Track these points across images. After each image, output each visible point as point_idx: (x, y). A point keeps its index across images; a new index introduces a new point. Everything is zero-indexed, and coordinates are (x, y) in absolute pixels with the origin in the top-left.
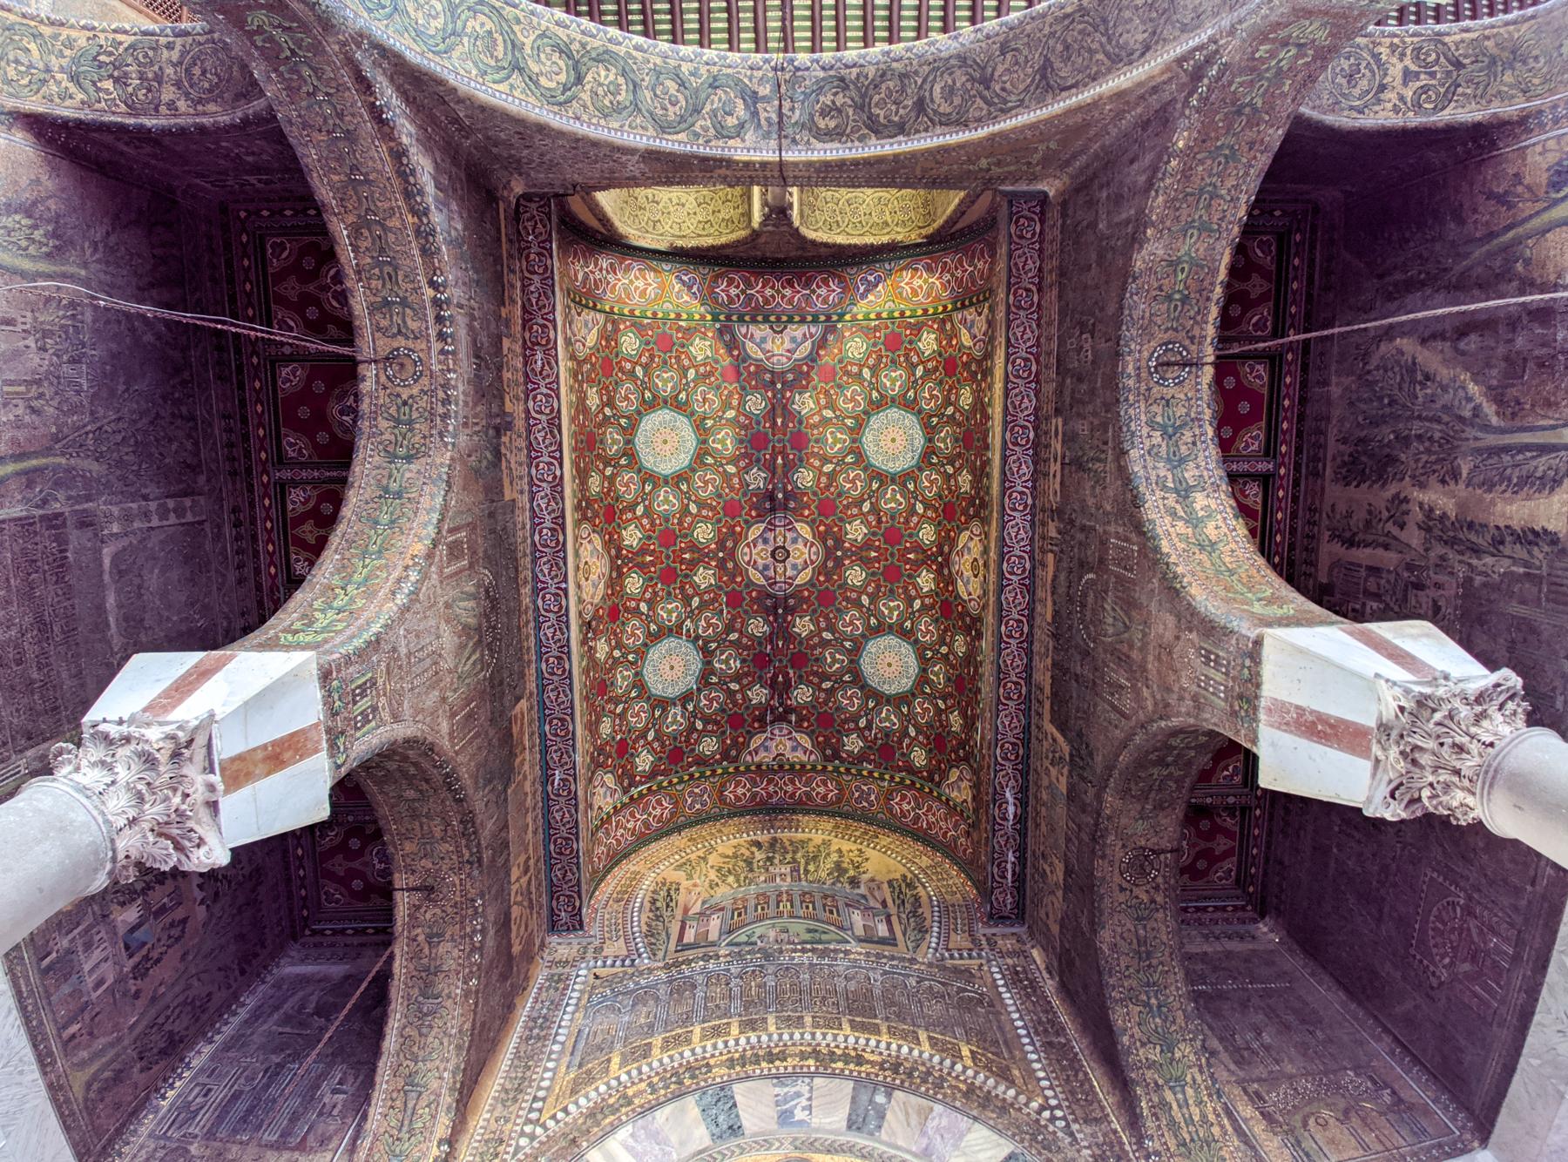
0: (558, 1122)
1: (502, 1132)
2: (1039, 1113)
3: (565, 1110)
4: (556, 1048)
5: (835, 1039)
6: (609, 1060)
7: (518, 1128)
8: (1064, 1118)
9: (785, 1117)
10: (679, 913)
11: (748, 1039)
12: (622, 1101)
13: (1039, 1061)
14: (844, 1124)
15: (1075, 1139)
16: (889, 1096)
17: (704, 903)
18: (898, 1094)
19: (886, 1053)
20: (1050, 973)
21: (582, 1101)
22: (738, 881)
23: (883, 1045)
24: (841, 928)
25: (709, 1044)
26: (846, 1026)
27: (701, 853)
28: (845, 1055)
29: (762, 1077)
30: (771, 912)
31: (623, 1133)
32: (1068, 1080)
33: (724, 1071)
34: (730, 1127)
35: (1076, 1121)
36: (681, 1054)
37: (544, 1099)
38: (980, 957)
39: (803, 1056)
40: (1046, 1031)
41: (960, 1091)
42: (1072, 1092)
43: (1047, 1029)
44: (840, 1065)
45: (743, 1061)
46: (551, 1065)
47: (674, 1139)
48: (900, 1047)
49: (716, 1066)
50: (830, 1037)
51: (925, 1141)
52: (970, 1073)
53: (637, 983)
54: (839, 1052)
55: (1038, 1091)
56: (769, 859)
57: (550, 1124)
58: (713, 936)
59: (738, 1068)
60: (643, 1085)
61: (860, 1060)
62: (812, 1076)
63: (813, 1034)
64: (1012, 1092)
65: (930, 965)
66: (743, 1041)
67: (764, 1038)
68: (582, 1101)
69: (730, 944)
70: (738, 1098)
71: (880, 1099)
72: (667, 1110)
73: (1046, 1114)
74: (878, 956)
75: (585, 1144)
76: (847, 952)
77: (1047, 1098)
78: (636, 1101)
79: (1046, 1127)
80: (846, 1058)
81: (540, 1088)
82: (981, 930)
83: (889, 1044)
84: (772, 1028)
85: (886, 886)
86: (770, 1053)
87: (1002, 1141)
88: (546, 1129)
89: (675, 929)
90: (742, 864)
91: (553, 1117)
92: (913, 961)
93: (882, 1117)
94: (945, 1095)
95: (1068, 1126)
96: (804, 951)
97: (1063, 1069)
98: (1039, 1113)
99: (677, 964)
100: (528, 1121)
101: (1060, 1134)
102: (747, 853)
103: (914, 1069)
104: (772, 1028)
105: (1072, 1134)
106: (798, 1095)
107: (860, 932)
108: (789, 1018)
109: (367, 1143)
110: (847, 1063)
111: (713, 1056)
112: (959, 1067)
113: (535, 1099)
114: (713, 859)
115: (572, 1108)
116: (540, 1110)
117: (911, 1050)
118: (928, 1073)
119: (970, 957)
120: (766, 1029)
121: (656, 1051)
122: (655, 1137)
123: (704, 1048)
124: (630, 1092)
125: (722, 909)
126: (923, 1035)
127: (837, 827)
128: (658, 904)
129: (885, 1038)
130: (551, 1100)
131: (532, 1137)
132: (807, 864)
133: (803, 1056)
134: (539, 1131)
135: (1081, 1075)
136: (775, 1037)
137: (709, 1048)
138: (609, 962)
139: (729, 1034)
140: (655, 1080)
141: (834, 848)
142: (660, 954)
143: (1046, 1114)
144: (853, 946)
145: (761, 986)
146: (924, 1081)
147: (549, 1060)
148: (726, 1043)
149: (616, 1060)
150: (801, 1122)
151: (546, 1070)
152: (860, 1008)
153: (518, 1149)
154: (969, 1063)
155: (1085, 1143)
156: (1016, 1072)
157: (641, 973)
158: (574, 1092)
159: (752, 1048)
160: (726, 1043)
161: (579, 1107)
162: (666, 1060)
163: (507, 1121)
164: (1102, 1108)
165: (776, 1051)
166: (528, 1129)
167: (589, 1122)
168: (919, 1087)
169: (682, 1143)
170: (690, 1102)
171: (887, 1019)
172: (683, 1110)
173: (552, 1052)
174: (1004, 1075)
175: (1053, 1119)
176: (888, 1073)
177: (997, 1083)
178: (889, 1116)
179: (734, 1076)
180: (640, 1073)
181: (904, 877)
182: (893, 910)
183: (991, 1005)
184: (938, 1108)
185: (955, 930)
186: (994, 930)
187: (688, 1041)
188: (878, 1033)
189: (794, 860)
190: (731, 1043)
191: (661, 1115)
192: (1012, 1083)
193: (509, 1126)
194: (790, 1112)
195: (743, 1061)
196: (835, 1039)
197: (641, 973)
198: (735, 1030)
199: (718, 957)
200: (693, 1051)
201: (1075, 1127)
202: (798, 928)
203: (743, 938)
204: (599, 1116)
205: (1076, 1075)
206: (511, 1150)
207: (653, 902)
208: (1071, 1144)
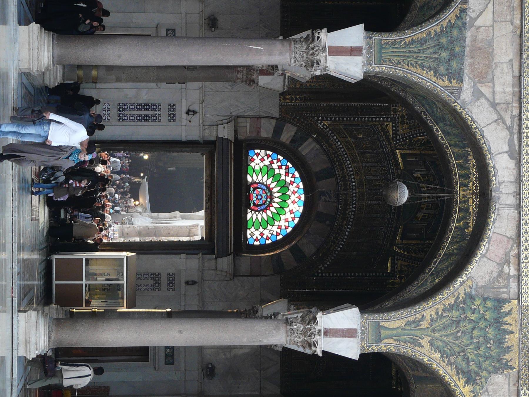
8: (318, 276)
9: (323, 193)
13: (340, 275)
31: (318, 146)
46: (345, 119)
49: (343, 173)
54: (347, 212)
64: (328, 263)
68: (330, 132)
70: (330, 179)
71: (328, 222)
73: (320, 271)
88: (320, 124)
89: (415, 152)
95: (315, 276)
100: (323, 118)
113: (331, 118)
115: (328, 130)
118: (337, 239)
134: (320, 122)
143: (320, 271)
151: (343, 119)
157: (389, 141)
161: (328, 132)
173: (350, 118)
175: (318, 273)
184: (323, 239)
191: (325, 157)
194: (324, 195)
197: (389, 141)
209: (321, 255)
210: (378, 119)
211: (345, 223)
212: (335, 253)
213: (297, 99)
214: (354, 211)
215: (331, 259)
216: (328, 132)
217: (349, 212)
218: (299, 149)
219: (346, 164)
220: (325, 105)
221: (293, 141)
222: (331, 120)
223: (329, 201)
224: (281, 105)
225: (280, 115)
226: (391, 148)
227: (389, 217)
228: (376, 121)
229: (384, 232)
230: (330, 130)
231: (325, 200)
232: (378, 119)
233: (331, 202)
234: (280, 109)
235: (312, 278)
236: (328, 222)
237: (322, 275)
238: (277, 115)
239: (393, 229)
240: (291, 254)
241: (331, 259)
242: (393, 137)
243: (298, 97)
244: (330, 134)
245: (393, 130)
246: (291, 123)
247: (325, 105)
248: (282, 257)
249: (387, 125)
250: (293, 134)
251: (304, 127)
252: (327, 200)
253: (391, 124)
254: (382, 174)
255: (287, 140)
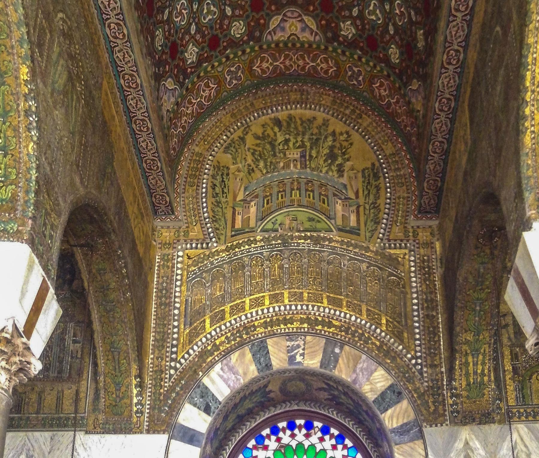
0: (186, 360)
1: (161, 366)
2: (410, 360)
3: (188, 353)
4: (176, 312)
5: (318, 310)
6: (204, 321)
7: (168, 364)
8: (421, 364)
9: (292, 359)
10: (230, 197)
11: (274, 308)
12: (214, 348)
13: (418, 328)
14: (319, 364)
15: (423, 377)
16: (341, 348)
17: (246, 189)
18: (347, 348)
19: (343, 320)
20: (441, 263)
21: (195, 348)
22: (266, 166)
23: (342, 315)
24: (329, 218)
25: (254, 311)
26: (325, 301)
27: (239, 133)
28: (323, 320)
29: (281, 334)
30: (287, 200)
32: (429, 341)
33: (262, 330)
34: (266, 365)
35: (426, 366)
36: (240, 318)
37: (176, 346)
38: (406, 248)
39: (302, 321)
40: (428, 307)
41: (376, 346)
42: (430, 349)
43: (429, 304)
44: (320, 327)
45: (272, 323)
46: (176, 324)
47: (241, 371)
48: (351, 316)
49: (258, 326)
50: (315, 308)
51: (354, 376)
52: (383, 334)
53: (212, 263)
54: (320, 319)
55: (413, 347)
56: (287, 141)
57: (183, 361)
58: (252, 223)
59: (269, 328)
60: (223, 338)
61: (330, 325)
62: (306, 334)
63: (307, 306)
65: (376, 253)
66: (271, 310)
67: (282, 308)
68: (195, 348)
69: (263, 231)
70: (270, 348)
71: (337, 350)
72: (237, 354)
74: (349, 244)
75: (201, 373)
76: (330, 240)
77: (416, 352)
78: (221, 348)
79: (411, 369)
80: (323, 323)
81: (174, 339)
82: (412, 222)
83: (346, 314)
84: (286, 301)
85: (360, 175)
86: (285, 319)
87: (389, 377)
88: (181, 364)
89: (229, 216)
90: (268, 146)
91: (183, 357)
92: (367, 249)
93: (337, 361)
94: (368, 348)
96: (306, 238)
97: (429, 333)
98: (410, 360)
99: (232, 248)
100: (172, 360)
101: (417, 373)
102: (272, 134)
103: (356, 331)
104: (286, 301)
105: (421, 373)
106: (298, 346)
107: (339, 222)
108: (295, 294)
109: (102, 378)
110: (323, 327)
111: (256, 319)
112: (378, 331)
113: (173, 346)
114: (250, 140)
115: (191, 351)
116: (176, 353)
117: (357, 318)
118: (363, 334)
119: (401, 248)
120: (283, 302)
121: (227, 315)
122: (231, 369)
123: (251, 313)
124: (218, 342)
125: (257, 197)
126: (364, 308)
127: (334, 102)
128: (218, 190)
129: (345, 310)
130: (180, 346)
131: (176, 369)
132: (311, 148)
133: (302, 321)
134: (178, 365)
135: (436, 339)
136: (288, 307)
137: (254, 314)
138: (194, 245)
139: (263, 304)
140: (229, 335)
141: (330, 129)
142: (223, 238)
144: (335, 235)
145: (281, 267)
146: (360, 339)
147: (175, 320)
148: (262, 310)
149: (208, 321)
150: (299, 363)
151: (174, 327)
152: (333, 284)
153: (171, 376)
154: (384, 328)
155: (426, 379)
156: (405, 335)
157: (213, 255)
158: (190, 342)
159: (276, 315)
160: (262, 310)
161: (194, 351)
162: (233, 322)
163: (162, 359)
164: (440, 358)
165: (288, 317)
166: (173, 364)
167: (201, 360)
168: (357, 342)
169: (245, 374)
170: (247, 349)
171: (347, 296)
172: (243, 355)
174: (399, 337)
175: (417, 364)
176: (343, 333)
177: (395, 341)
178: (340, 361)
179: (267, 334)
180: (221, 330)
181: (373, 165)
182: (361, 201)
183: (404, 287)
184: (364, 357)
185: (396, 222)
186: (420, 223)
187: (243, 309)
188: (341, 306)
189: (303, 146)
190: (265, 311)
191: (234, 357)
192: (402, 342)
193: (164, 362)
195: (272, 323)
196: (318, 310)
198: (267, 302)
199: (255, 241)
200: (246, 315)
201: (425, 369)
202: (303, 214)
203: (270, 226)
204: (205, 357)
205: (434, 338)
206: (167, 376)
207: (214, 186)
208: (420, 380)
209: (389, 361)
210: (179, 272)
211: (337, 323)
212: (384, 338)
213: (139, 403)
214: (319, 307)
215: (393, 344)
216: (194, 351)
217: (319, 315)
218: (221, 399)
219: (246, 321)
220: (152, 356)
221: (207, 410)
222: (176, 346)
223: (304, 349)
224: (148, 432)
225: (164, 433)
226: (223, 251)
227: (326, 254)
228: (182, 275)
229: (349, 260)
230: (192, 348)
231: (303, 355)
232: (179, 272)
233: (304, 344)
234: (154, 433)
235: (425, 375)
236: (337, 350)
237: (420, 357)
238: (165, 437)
239: (345, 247)
240: (389, 412)
241: (393, 344)
242: (207, 248)
243: (135, 400)
244: (198, 347)
245: (196, 248)
246: (178, 413)
247: (152, 356)
248: (395, 426)
249: (189, 258)
250: (196, 409)
251: (185, 393)
252: (301, 351)
253: (187, 251)
254: (262, 265)
255: (205, 421)
